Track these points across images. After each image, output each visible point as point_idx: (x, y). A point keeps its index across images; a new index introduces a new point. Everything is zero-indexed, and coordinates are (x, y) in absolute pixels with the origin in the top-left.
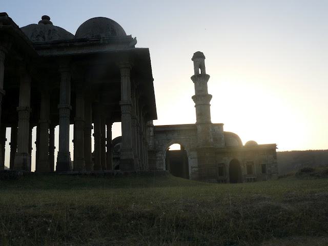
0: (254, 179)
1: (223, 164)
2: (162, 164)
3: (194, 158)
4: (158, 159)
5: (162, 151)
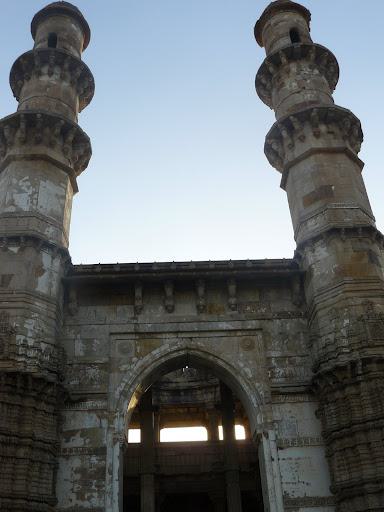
2: (101, 473)
4: (78, 442)
5: (104, 396)
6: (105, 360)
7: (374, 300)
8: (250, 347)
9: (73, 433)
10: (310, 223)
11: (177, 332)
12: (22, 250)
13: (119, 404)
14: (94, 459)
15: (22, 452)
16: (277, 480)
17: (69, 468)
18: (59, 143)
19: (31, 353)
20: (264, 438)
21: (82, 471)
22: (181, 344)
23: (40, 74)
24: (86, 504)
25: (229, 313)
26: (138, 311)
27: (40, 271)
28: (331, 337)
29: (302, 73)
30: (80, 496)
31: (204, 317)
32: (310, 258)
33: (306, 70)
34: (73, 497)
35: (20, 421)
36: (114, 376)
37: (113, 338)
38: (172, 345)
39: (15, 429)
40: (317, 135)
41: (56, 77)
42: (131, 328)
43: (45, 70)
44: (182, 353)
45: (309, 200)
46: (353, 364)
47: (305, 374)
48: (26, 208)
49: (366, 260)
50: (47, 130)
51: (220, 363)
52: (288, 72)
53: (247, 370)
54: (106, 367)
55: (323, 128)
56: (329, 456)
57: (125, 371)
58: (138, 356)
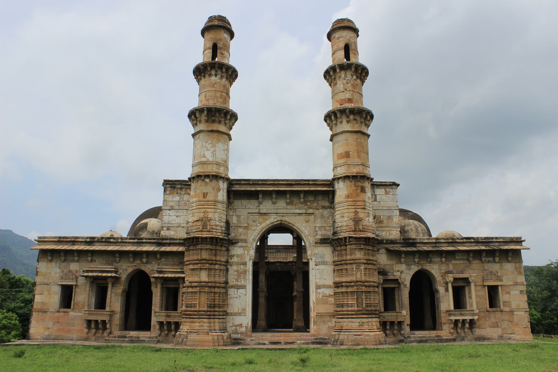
0: (472, 321)
1: (396, 281)
2: (245, 272)
3: (324, 263)
4: (235, 259)
5: (245, 241)
6: (246, 225)
7: (358, 210)
8: (307, 222)
9: (233, 256)
10: (339, 169)
11: (277, 213)
12: (211, 181)
13: (252, 244)
14: (242, 266)
15: (217, 267)
16: (314, 277)
17: (232, 270)
18: (223, 119)
19: (218, 228)
20: (310, 261)
21: (237, 271)
22: (279, 218)
23: (210, 75)
24: (239, 284)
25: (300, 205)
26: (260, 203)
27: (219, 190)
28: (340, 224)
29: (347, 78)
30: (237, 280)
31: (289, 207)
32: (336, 186)
33: (349, 77)
34: (234, 280)
35: (215, 255)
36: (250, 232)
37: (249, 215)
38: (274, 219)
39: (214, 258)
40: (348, 122)
41: (219, 76)
42: (257, 211)
43: (213, 72)
44: (279, 222)
45: (340, 156)
46: (345, 238)
47: (329, 234)
48: (211, 159)
49: (359, 191)
50: (217, 114)
51: (295, 227)
52: (340, 77)
53: (306, 231)
54: (246, 228)
55: (352, 117)
56: (334, 271)
57: (254, 230)
58: (260, 223)
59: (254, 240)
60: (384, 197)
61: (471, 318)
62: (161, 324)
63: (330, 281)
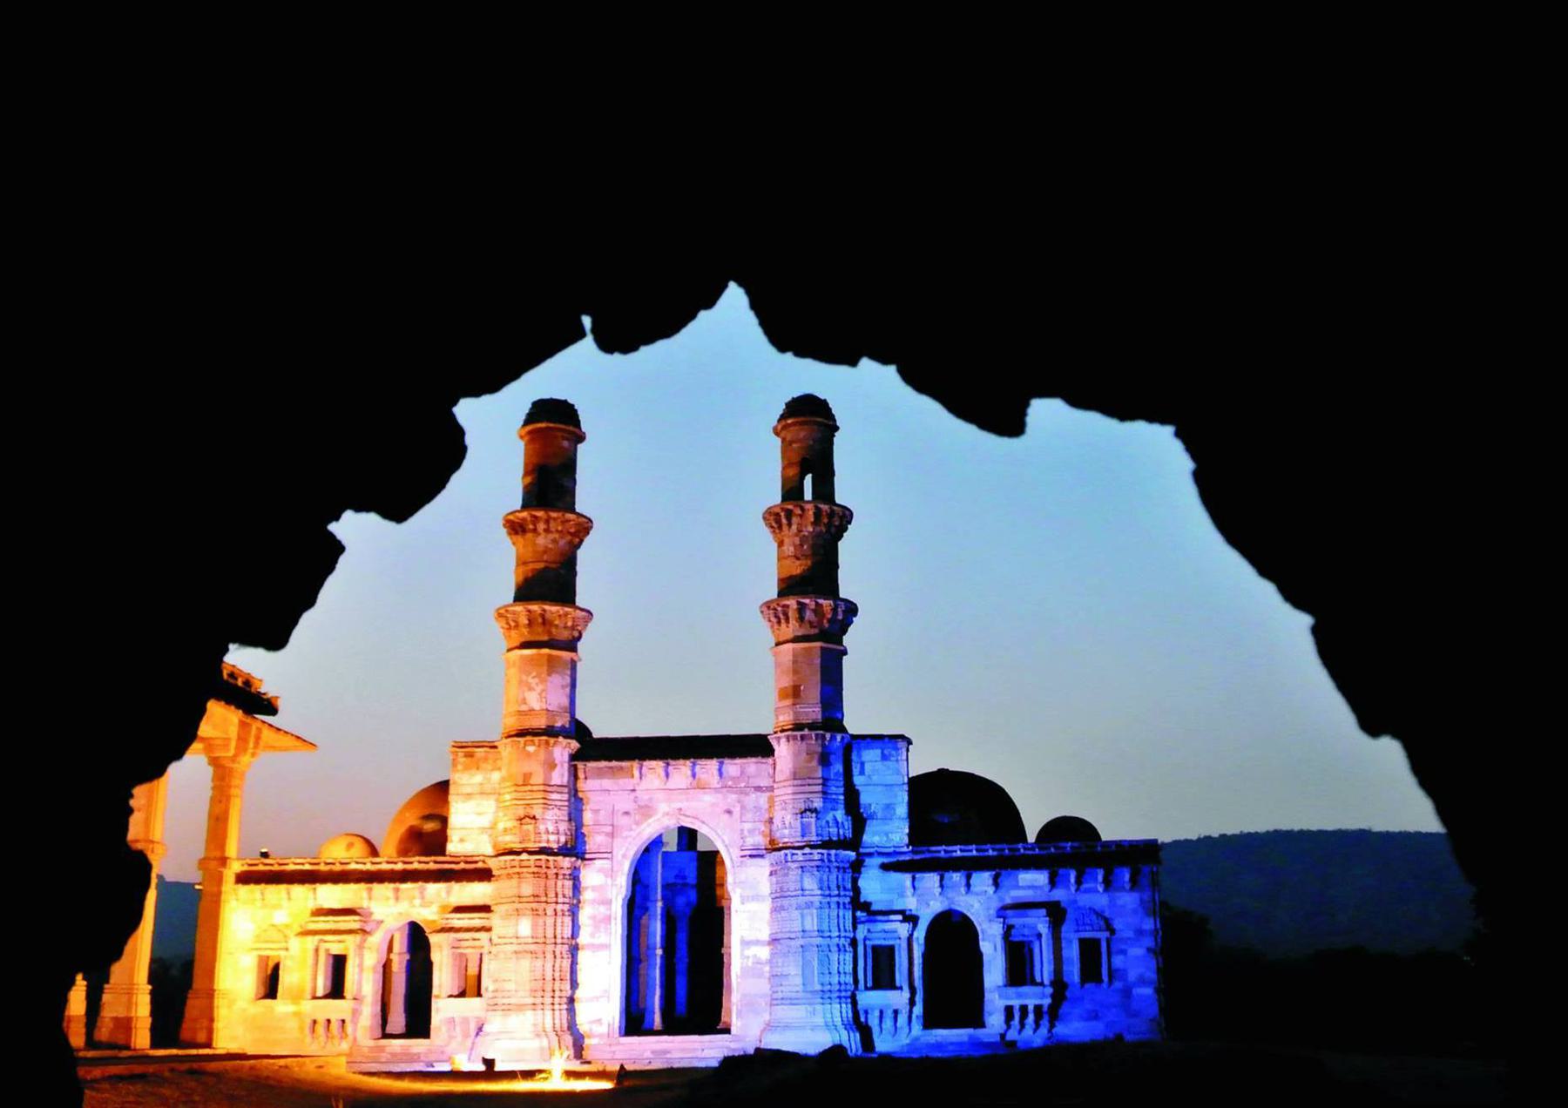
2: (608, 919)
3: (756, 898)
21: (593, 918)
36: (617, 842)
59: (624, 856)
60: (879, 765)
61: (1038, 1002)
62: (451, 1021)
63: (765, 935)
